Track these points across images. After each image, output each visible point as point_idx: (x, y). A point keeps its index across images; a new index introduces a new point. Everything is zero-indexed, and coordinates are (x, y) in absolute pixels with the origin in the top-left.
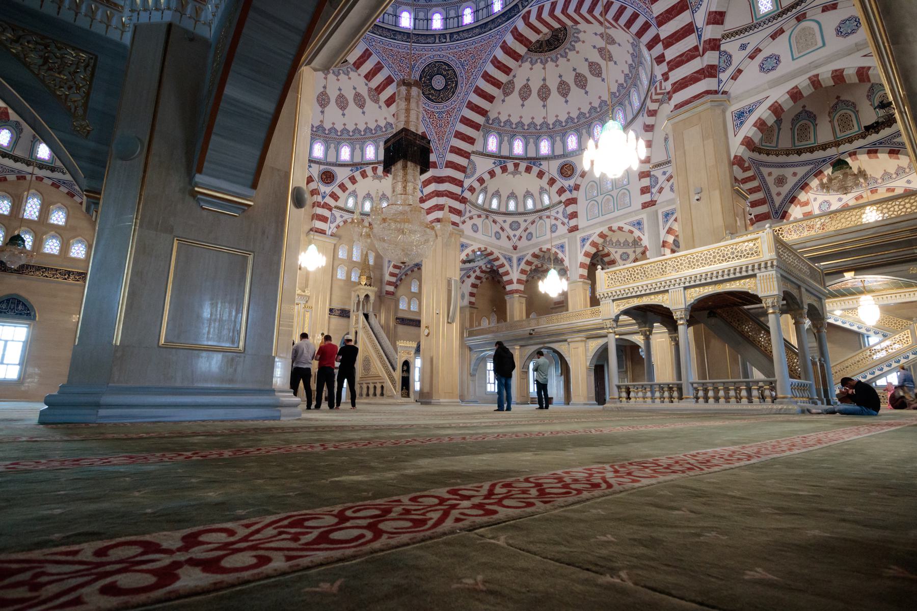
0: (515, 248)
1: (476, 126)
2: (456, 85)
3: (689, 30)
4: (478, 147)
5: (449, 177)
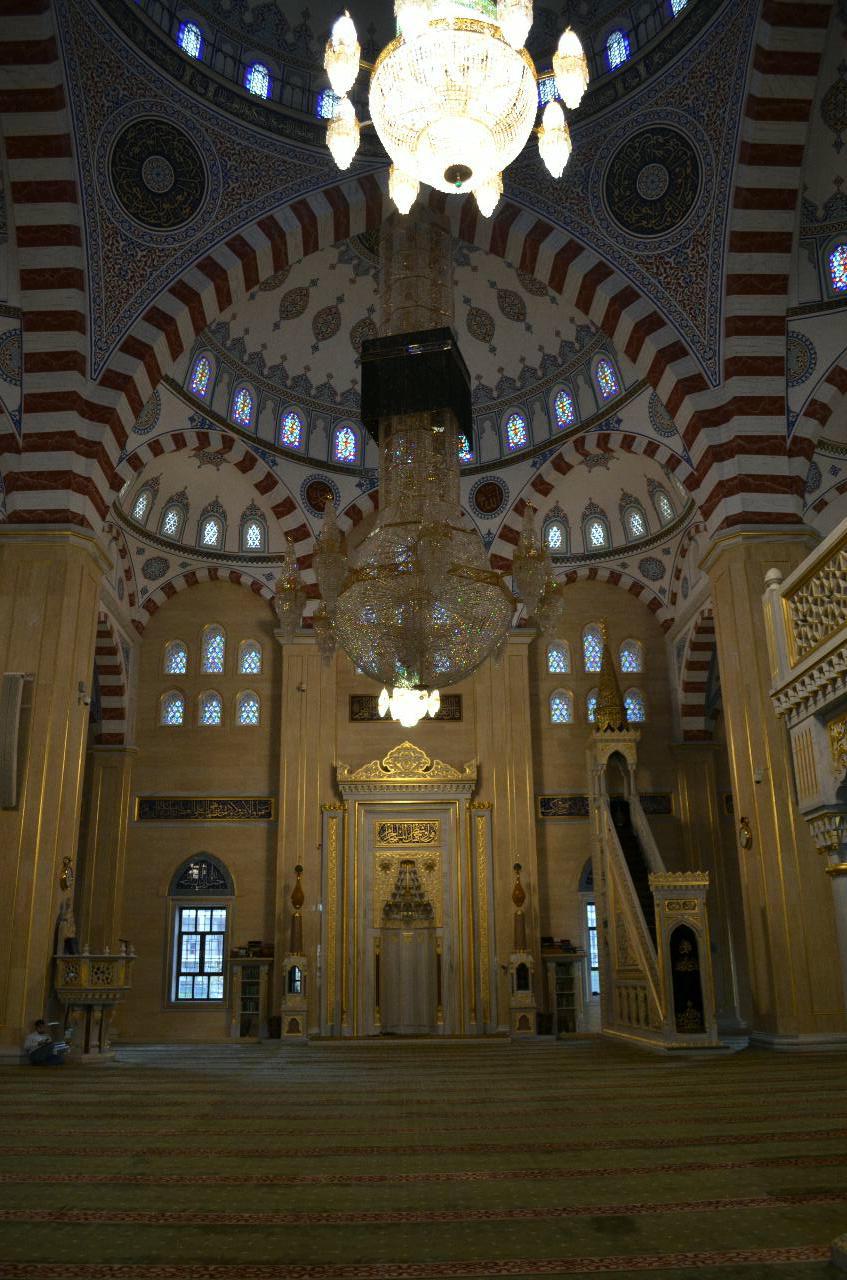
1: (777, 243)
2: (695, 167)
4: (804, 291)
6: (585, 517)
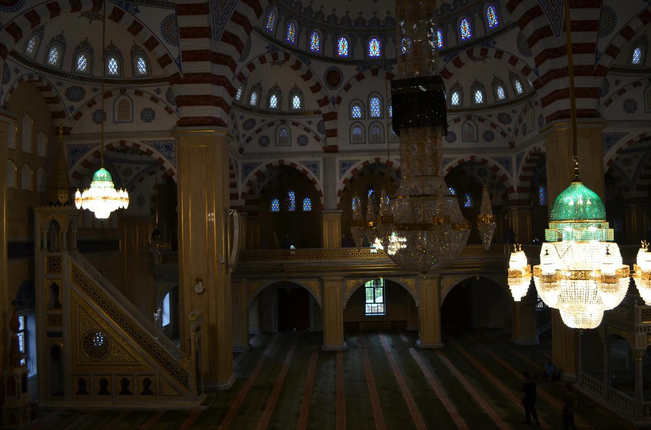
0: (241, 150)
3: (589, 48)
5: (229, 57)
6: (53, 41)
